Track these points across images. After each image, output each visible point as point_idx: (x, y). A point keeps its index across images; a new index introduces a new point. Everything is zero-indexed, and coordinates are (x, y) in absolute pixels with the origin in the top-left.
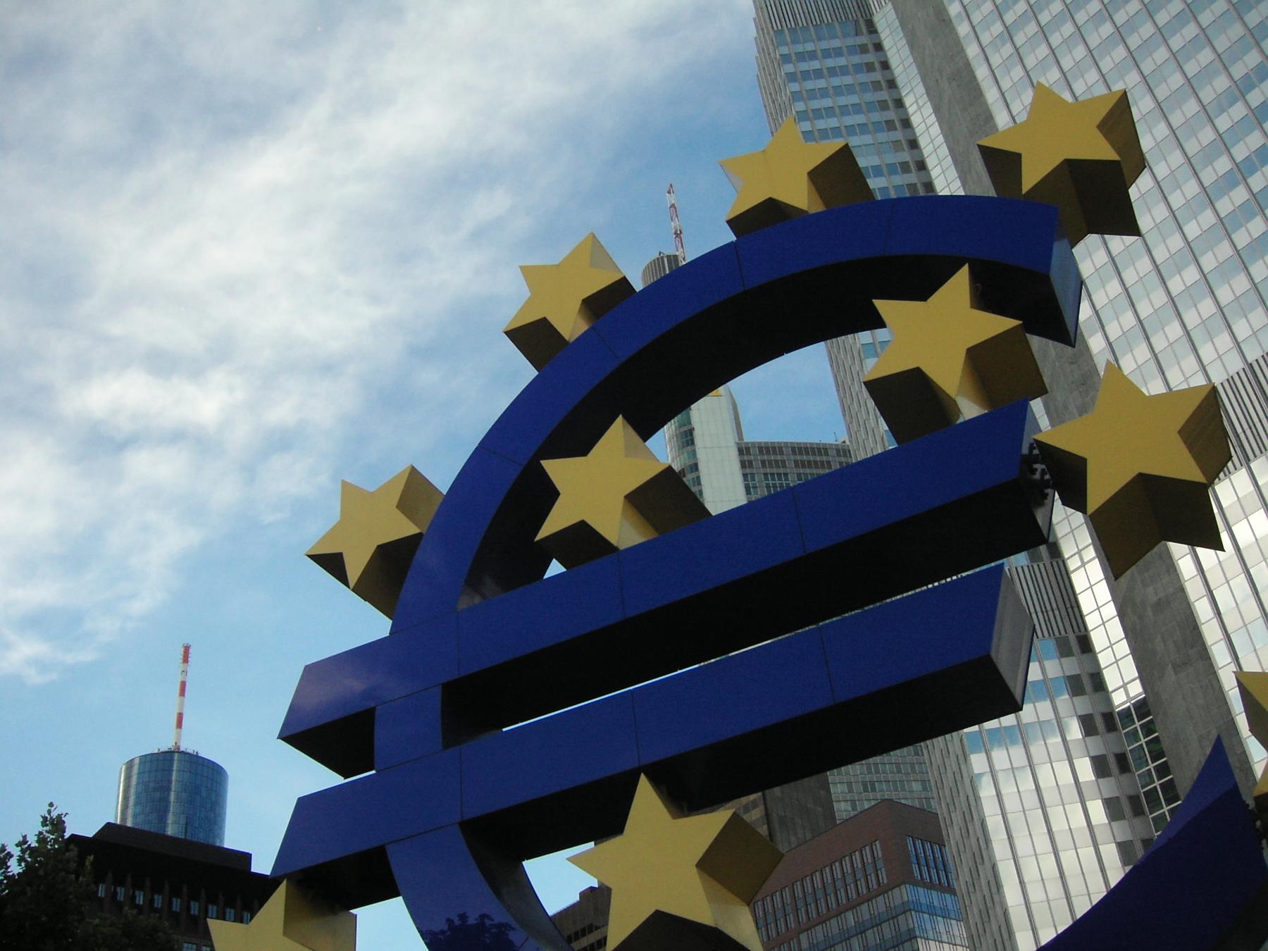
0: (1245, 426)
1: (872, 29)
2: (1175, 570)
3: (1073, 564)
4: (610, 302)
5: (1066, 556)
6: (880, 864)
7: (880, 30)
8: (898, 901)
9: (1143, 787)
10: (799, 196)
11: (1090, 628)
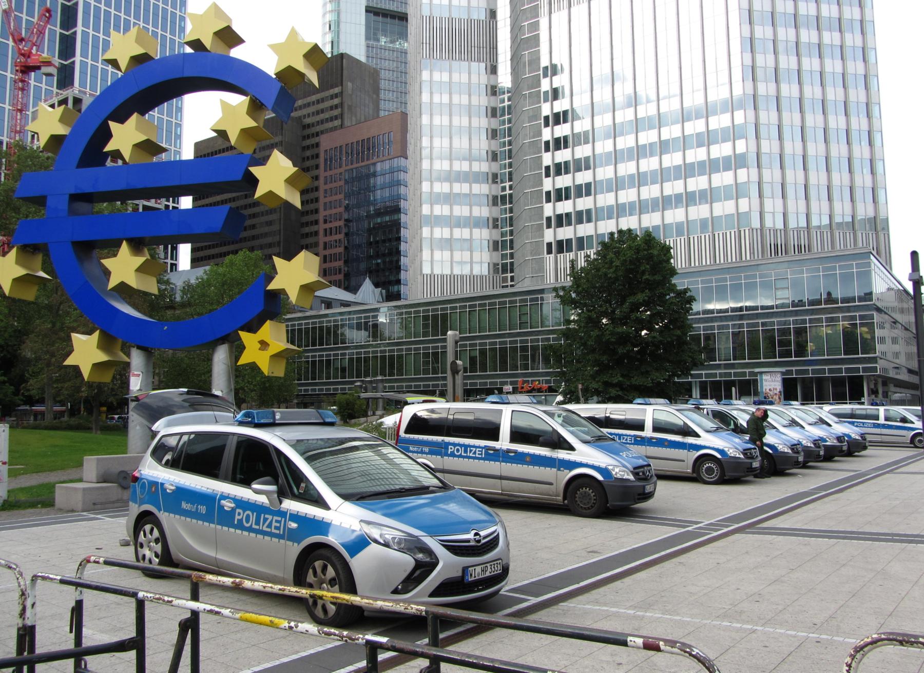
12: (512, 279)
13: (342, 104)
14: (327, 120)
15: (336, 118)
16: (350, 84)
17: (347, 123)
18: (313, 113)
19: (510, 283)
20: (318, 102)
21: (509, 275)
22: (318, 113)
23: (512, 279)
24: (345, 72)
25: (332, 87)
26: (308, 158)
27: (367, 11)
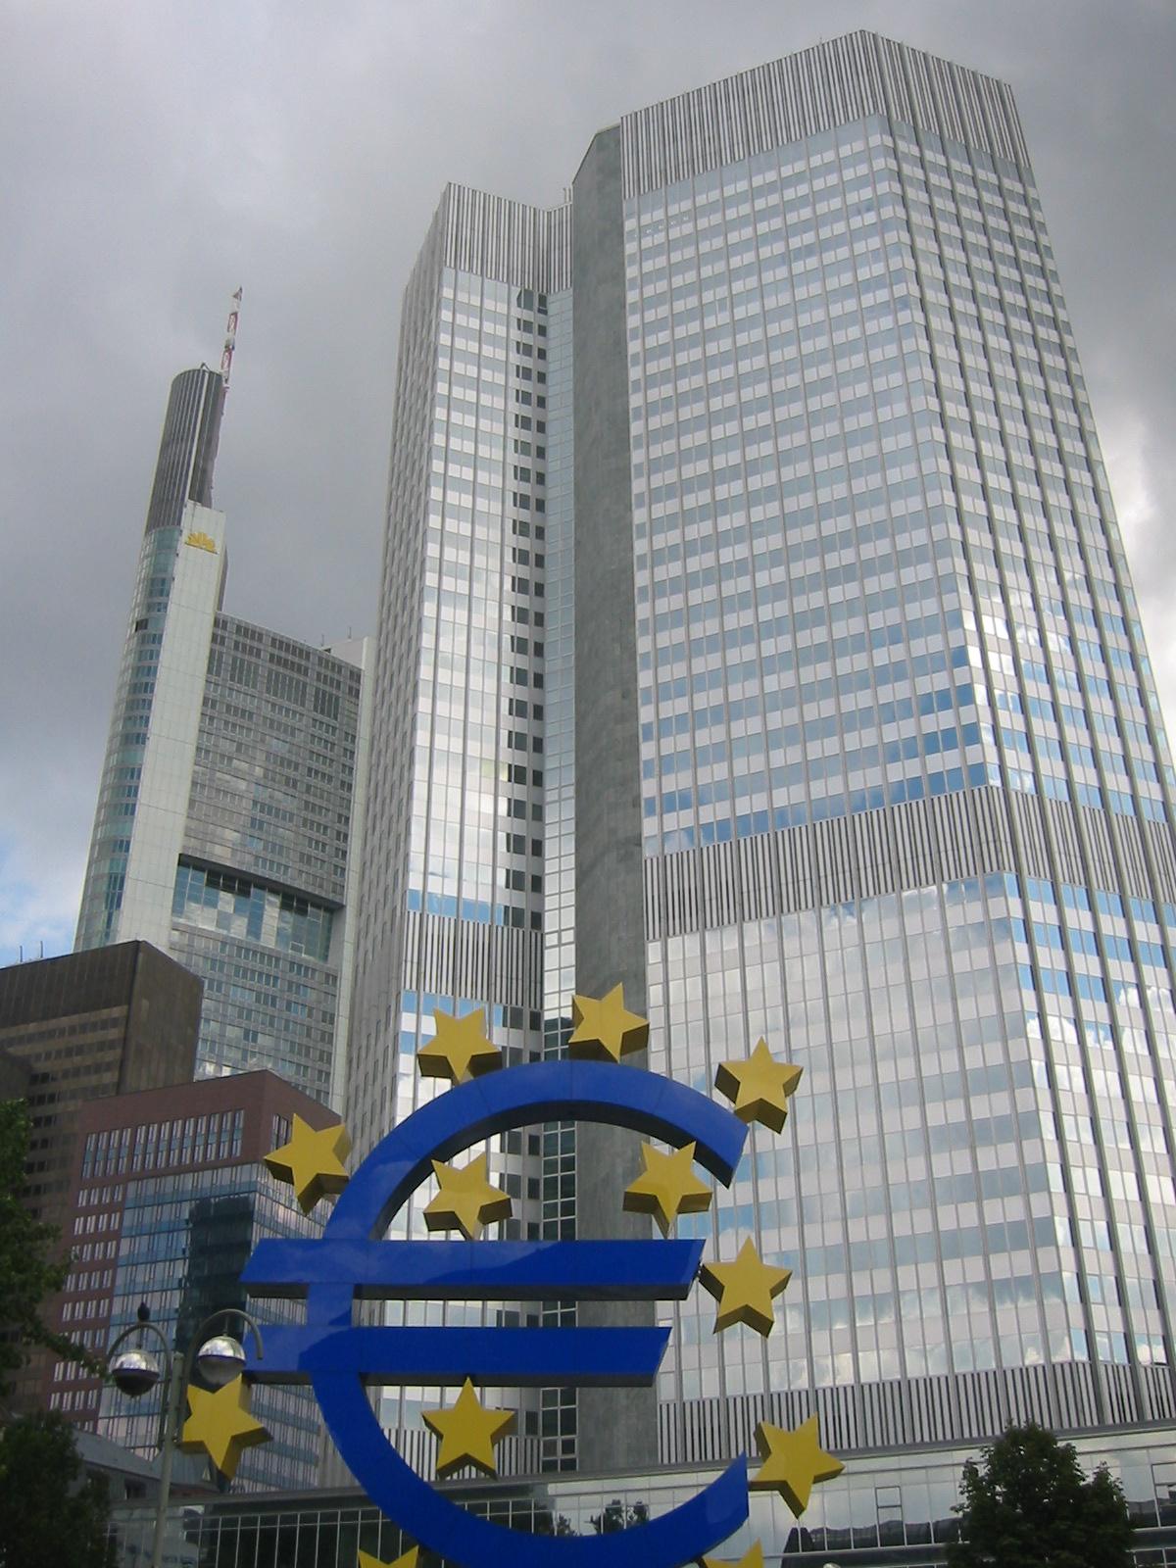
2: (645, 993)
3: (551, 940)
5: (546, 931)
6: (238, 1135)
7: (550, 313)
8: (245, 1179)
9: (545, 1173)
10: (613, 1046)
11: (546, 1007)
12: (568, 1446)
13: (125, 1041)
14: (88, 1070)
15: (109, 1067)
16: (145, 1003)
18: (59, 1052)
19: (560, 1456)
20: (73, 1030)
21: (559, 1439)
22: (69, 1052)
23: (568, 1446)
24: (139, 978)
25: (108, 1005)
27: (180, 864)
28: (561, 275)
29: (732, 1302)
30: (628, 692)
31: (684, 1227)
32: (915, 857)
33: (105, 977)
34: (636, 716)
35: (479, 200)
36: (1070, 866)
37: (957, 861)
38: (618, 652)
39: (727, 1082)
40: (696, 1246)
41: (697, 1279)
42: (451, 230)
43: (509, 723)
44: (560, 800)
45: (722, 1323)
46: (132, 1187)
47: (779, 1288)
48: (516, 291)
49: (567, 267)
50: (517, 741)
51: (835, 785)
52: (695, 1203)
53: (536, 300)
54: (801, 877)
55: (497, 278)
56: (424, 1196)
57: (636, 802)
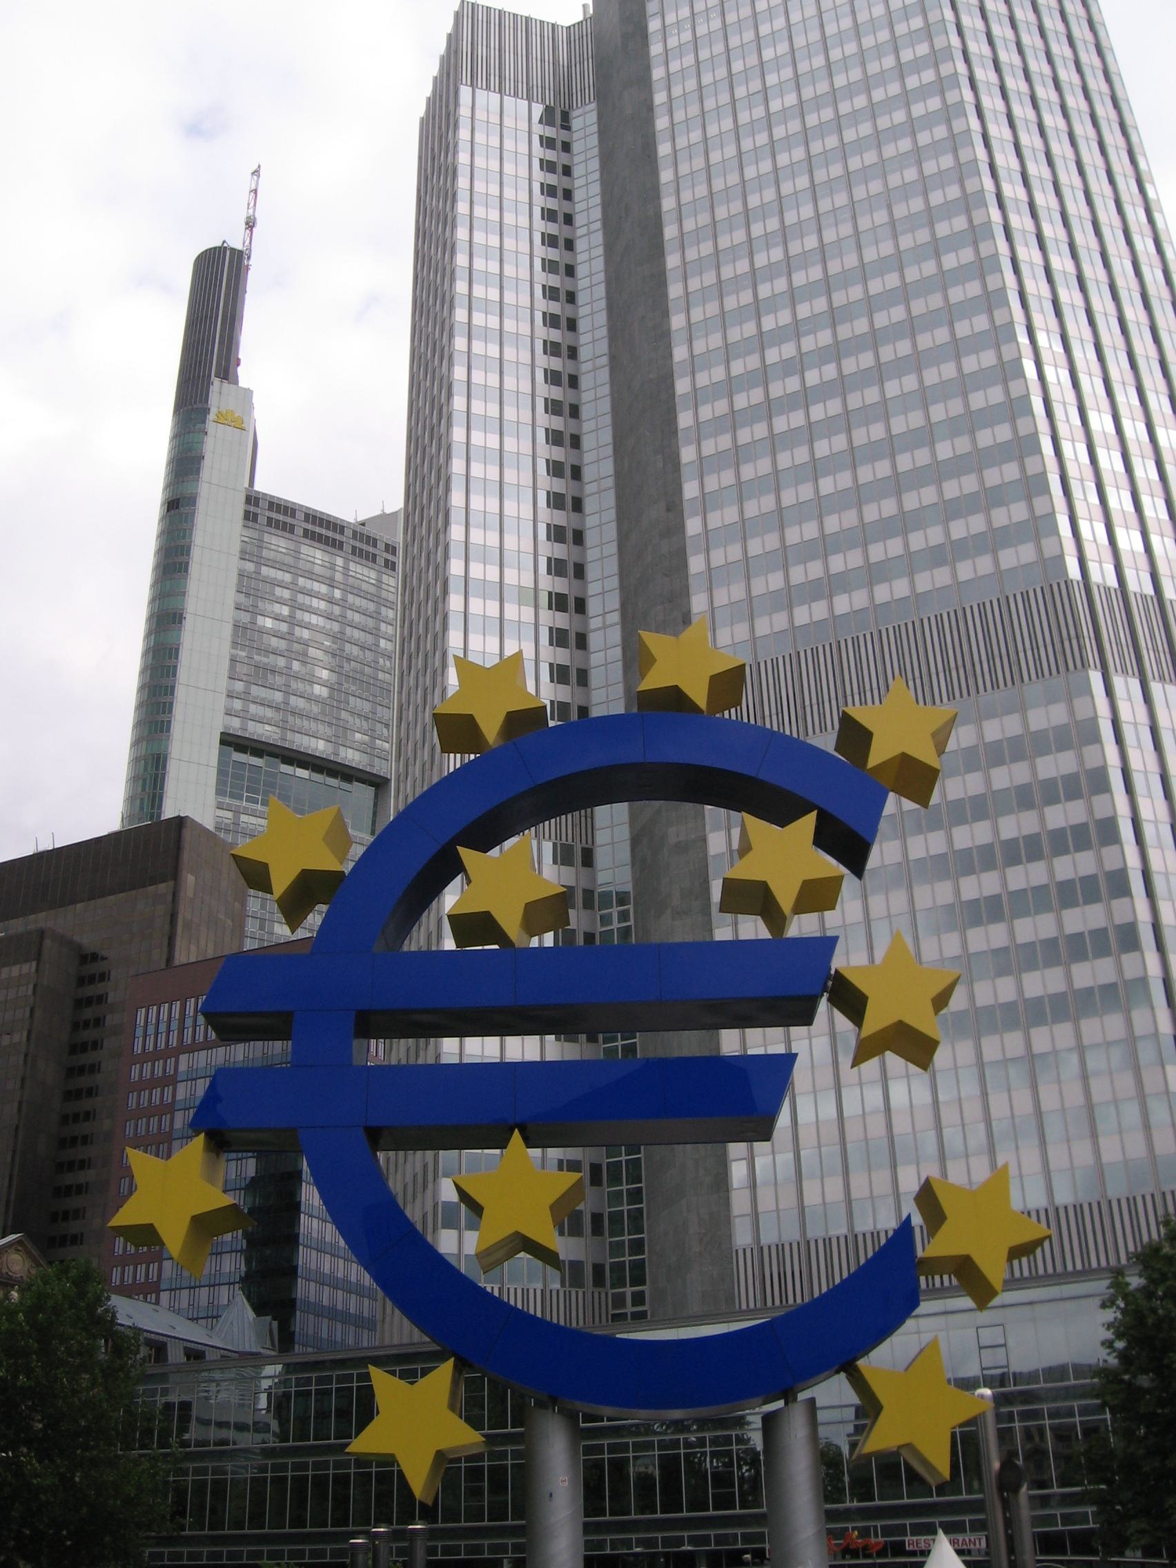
0: (814, 701)
1: (566, 127)
4: (524, 721)
7: (574, 128)
10: (699, 695)
12: (639, 1299)
17: (180, 957)
19: (629, 1309)
21: (629, 1290)
23: (639, 1299)
25: (154, 881)
26: (86, 1024)
28: (583, 90)
29: (875, 1020)
30: (674, 505)
31: (802, 926)
32: (990, 658)
33: (146, 852)
34: (682, 527)
35: (494, 19)
36: (1158, 662)
37: (1037, 660)
38: (660, 465)
39: (854, 736)
40: (827, 944)
41: (826, 995)
42: (466, 47)
43: (548, 549)
44: (605, 627)
45: (865, 1050)
46: (183, 1058)
47: (940, 1001)
48: (538, 110)
49: (590, 79)
50: (555, 438)
51: (901, 588)
52: (818, 896)
53: (558, 116)
54: (868, 687)
55: (516, 95)
56: (451, 898)
57: (686, 620)
